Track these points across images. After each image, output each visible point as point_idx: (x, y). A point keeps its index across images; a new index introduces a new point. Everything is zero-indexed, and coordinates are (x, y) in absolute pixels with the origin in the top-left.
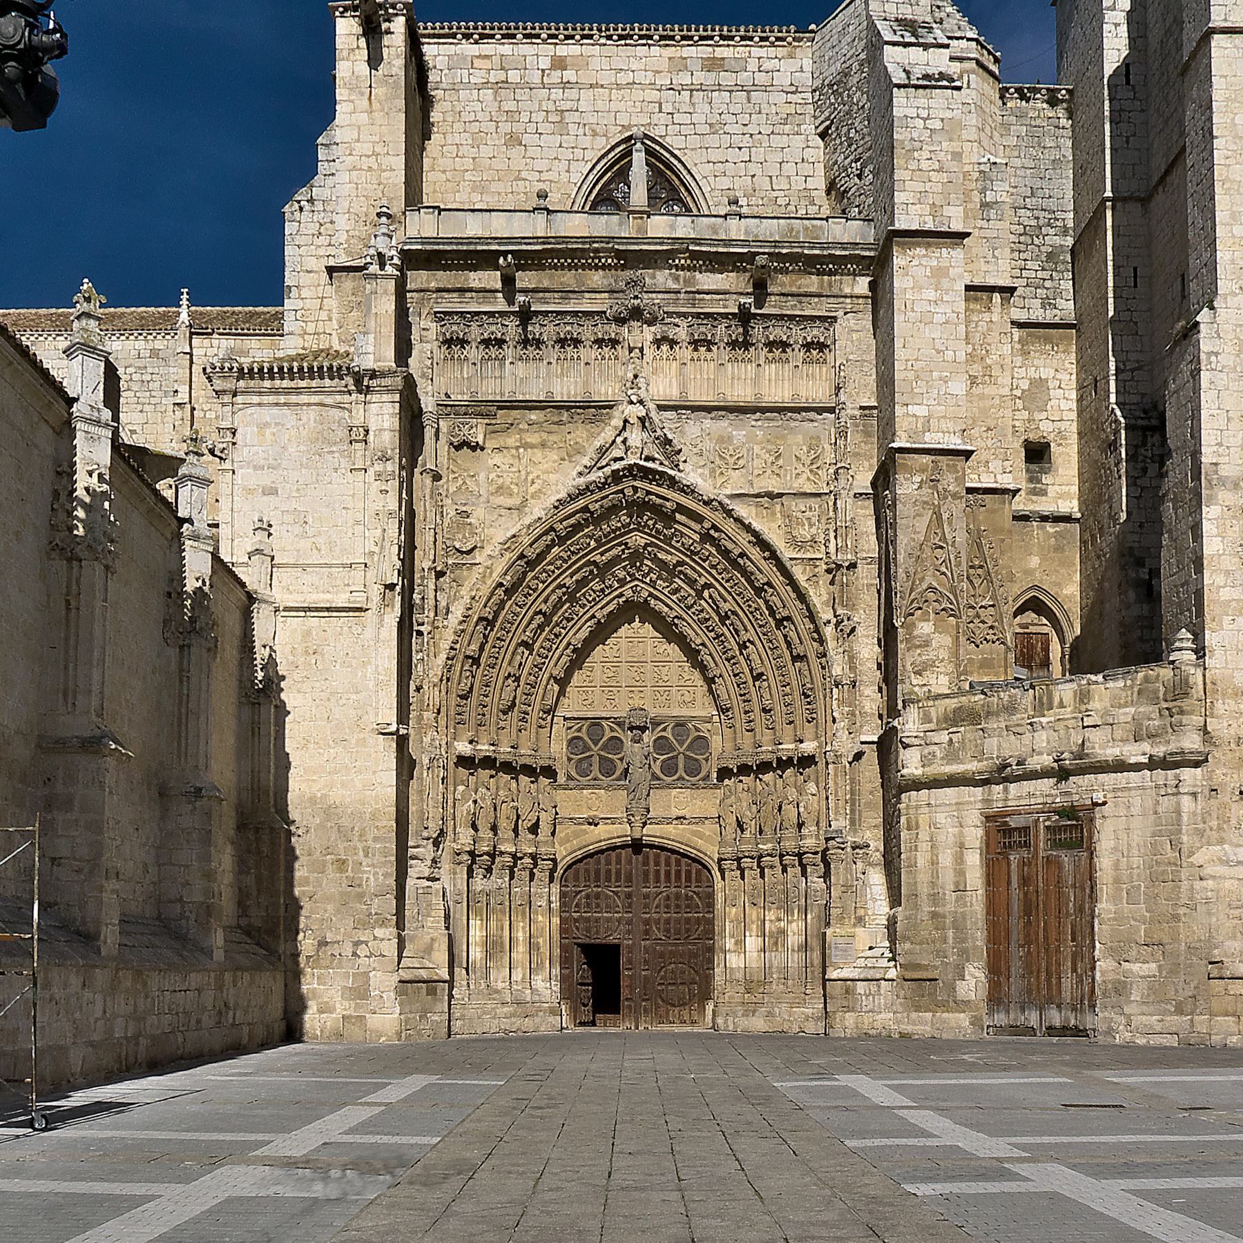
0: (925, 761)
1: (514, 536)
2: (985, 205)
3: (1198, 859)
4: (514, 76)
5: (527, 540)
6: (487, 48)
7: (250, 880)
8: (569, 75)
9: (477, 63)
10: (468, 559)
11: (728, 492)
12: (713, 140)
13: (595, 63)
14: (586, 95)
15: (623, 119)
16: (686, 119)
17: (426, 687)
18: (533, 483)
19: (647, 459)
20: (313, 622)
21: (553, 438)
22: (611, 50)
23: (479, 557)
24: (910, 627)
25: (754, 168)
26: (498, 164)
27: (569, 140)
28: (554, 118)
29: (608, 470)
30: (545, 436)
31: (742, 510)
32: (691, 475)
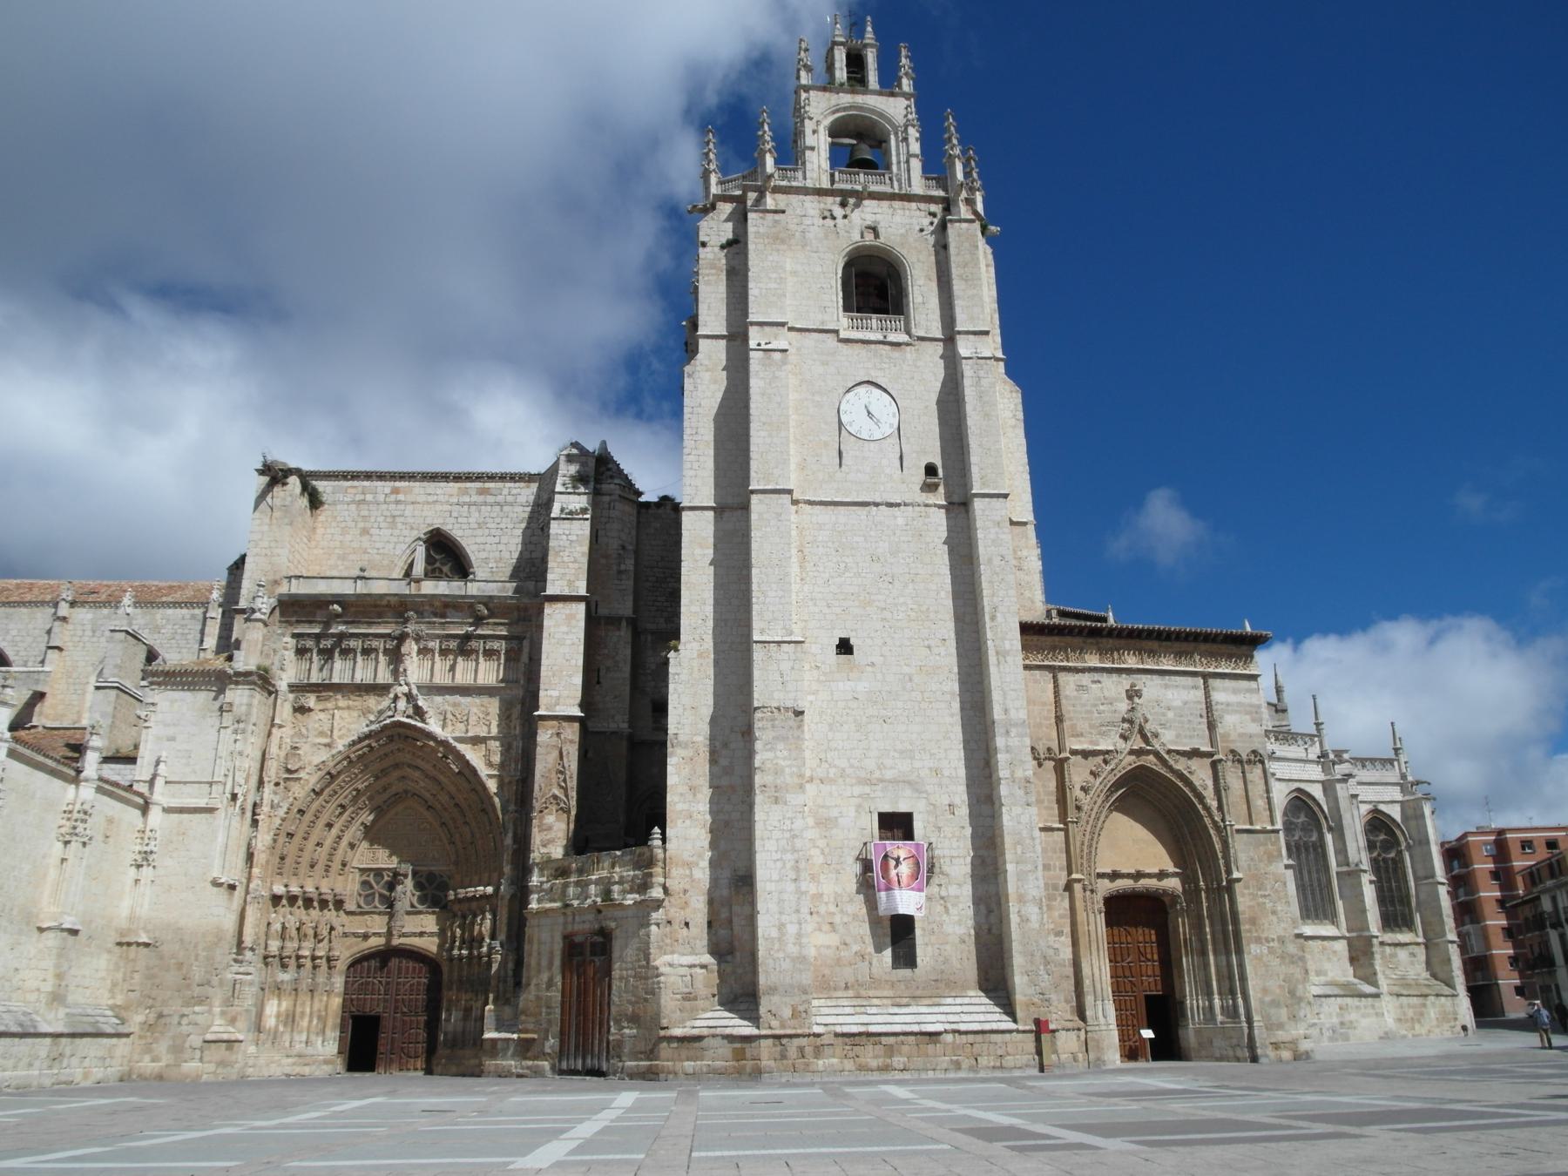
0: (539, 901)
1: (323, 762)
2: (620, 572)
3: (657, 963)
4: (369, 497)
5: (332, 764)
6: (355, 483)
7: (120, 976)
8: (401, 497)
9: (349, 490)
10: (295, 776)
11: (454, 735)
12: (479, 532)
13: (416, 491)
14: (410, 507)
15: (429, 521)
16: (465, 520)
17: (256, 853)
18: (340, 730)
19: (408, 717)
20: (185, 816)
21: (355, 703)
22: (425, 484)
23: (302, 774)
24: (541, 819)
25: (501, 547)
26: (355, 545)
27: (397, 532)
28: (389, 520)
29: (382, 724)
30: (351, 702)
31: (463, 748)
32: (433, 726)
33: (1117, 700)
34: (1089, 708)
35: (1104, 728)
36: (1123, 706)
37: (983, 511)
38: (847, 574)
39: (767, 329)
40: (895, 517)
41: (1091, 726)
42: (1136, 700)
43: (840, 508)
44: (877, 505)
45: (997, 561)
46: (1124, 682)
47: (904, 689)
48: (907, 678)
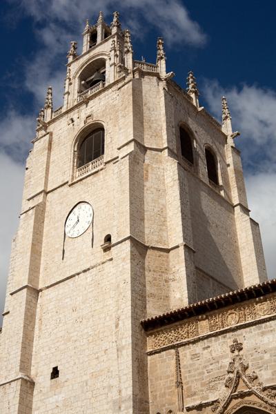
33: (222, 357)
34: (200, 371)
35: (212, 384)
36: (227, 361)
37: (117, 254)
38: (60, 325)
39: (35, 198)
40: (86, 278)
41: (203, 385)
42: (236, 352)
43: (60, 284)
44: (78, 274)
45: (122, 285)
46: (229, 340)
47: (83, 392)
48: (85, 384)
